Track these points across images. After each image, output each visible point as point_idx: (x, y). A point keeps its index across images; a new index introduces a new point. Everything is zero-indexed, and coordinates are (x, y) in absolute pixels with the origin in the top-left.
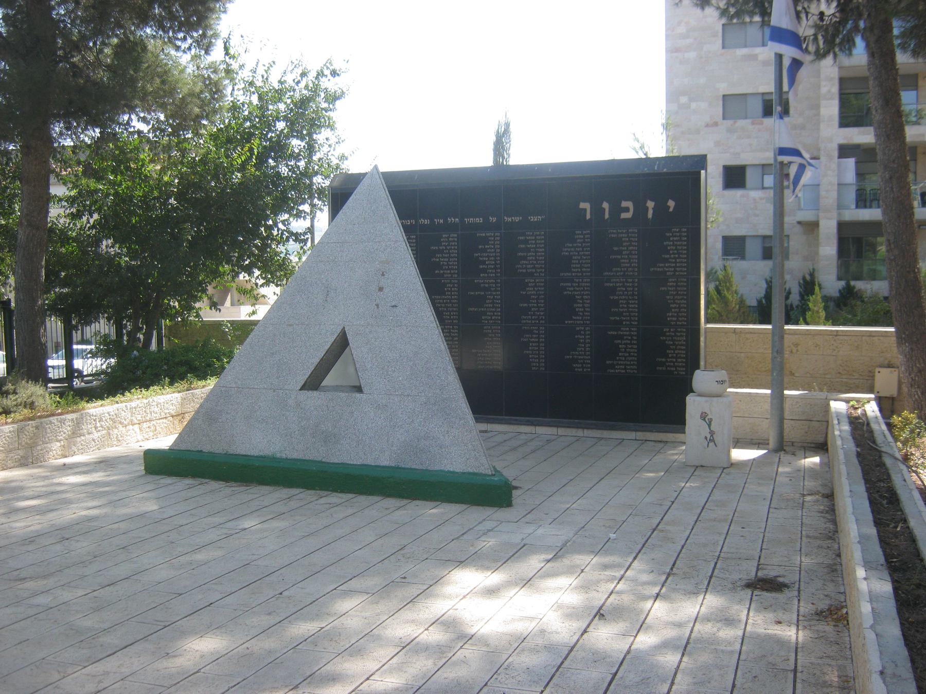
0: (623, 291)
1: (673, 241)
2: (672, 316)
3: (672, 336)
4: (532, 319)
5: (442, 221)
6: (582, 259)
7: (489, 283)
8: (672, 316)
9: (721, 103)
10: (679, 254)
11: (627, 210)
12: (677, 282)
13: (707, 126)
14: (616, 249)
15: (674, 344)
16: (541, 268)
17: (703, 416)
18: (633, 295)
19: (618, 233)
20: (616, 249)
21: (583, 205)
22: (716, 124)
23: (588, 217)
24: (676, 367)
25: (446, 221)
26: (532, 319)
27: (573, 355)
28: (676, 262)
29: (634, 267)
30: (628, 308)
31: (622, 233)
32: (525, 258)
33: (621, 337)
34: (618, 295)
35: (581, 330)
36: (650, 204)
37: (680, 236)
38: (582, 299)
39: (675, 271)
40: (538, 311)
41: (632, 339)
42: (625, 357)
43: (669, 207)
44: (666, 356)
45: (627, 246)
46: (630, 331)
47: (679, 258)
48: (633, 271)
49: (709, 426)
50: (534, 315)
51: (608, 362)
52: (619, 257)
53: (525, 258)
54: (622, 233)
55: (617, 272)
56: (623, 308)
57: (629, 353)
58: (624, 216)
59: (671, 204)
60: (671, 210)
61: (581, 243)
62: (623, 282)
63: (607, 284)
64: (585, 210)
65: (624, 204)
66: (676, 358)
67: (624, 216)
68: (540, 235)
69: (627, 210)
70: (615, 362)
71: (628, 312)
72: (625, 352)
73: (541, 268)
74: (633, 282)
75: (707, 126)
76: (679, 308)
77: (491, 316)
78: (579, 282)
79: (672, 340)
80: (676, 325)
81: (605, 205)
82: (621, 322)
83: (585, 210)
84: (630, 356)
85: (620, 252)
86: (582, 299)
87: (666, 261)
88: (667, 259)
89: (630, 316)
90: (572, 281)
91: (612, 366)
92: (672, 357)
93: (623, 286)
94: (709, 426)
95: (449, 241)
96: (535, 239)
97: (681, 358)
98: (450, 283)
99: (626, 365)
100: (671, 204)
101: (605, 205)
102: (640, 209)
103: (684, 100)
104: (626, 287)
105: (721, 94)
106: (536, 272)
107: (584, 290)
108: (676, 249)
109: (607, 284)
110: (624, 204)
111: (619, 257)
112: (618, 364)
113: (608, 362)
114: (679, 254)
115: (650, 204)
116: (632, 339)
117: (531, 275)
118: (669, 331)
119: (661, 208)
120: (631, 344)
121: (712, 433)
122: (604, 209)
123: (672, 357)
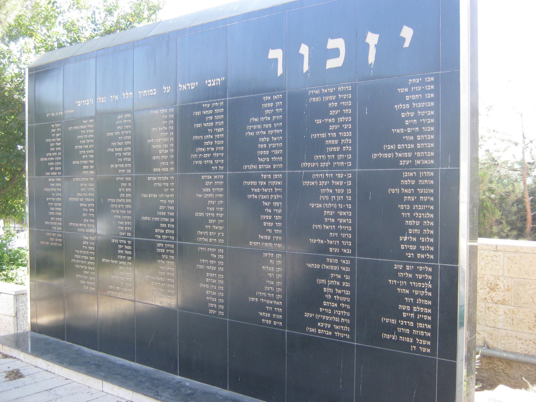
0: (330, 195)
1: (410, 102)
2: (409, 242)
3: (408, 280)
4: (209, 237)
6: (271, 141)
7: (162, 181)
8: (409, 242)
11: (335, 53)
14: (319, 121)
15: (411, 295)
16: (220, 158)
18: (345, 202)
19: (322, 95)
20: (319, 121)
23: (280, 71)
24: (414, 337)
26: (209, 237)
27: (259, 297)
28: (415, 142)
29: (347, 152)
30: (337, 223)
31: (329, 94)
32: (200, 143)
33: (325, 274)
34: (322, 202)
35: (269, 258)
36: (372, 39)
37: (423, 92)
38: (271, 207)
40: (216, 224)
41: (342, 280)
42: (333, 309)
43: (404, 40)
44: (398, 315)
45: (336, 117)
46: (340, 264)
47: (421, 132)
48: (345, 160)
50: (212, 230)
51: (307, 315)
52: (323, 135)
53: (200, 143)
54: (329, 94)
55: (320, 161)
56: (329, 223)
57: (339, 302)
58: (332, 63)
59: (407, 33)
60: (407, 44)
61: (270, 115)
62: (330, 179)
63: (306, 183)
64: (276, 60)
65: (332, 44)
66: (415, 321)
67: (332, 63)
68: (219, 107)
69: (335, 53)
70: (318, 316)
71: (337, 230)
72: (333, 300)
73: (220, 158)
74: (345, 179)
76: (422, 227)
77: (164, 229)
78: (267, 180)
79: (408, 287)
80: (415, 258)
81: (304, 50)
82: (324, 249)
83: (276, 60)
84: (339, 308)
85: (325, 128)
86: (271, 207)
88: (401, 135)
89: (340, 239)
90: (258, 178)
91: (313, 322)
92: (408, 319)
93: (330, 186)
96: (213, 114)
97: (422, 321)
98: (124, 181)
99: (333, 323)
100: (407, 33)
101: (304, 50)
102: (356, 48)
104: (334, 187)
106: (214, 164)
107: (274, 193)
108: (416, 117)
109: (306, 183)
110: (332, 44)
111: (323, 135)
112: (321, 320)
113: (307, 315)
115: (372, 39)
116: (342, 280)
117: (207, 168)
118: (404, 270)
119: (390, 43)
120: (341, 287)
122: (302, 56)
123: (408, 319)
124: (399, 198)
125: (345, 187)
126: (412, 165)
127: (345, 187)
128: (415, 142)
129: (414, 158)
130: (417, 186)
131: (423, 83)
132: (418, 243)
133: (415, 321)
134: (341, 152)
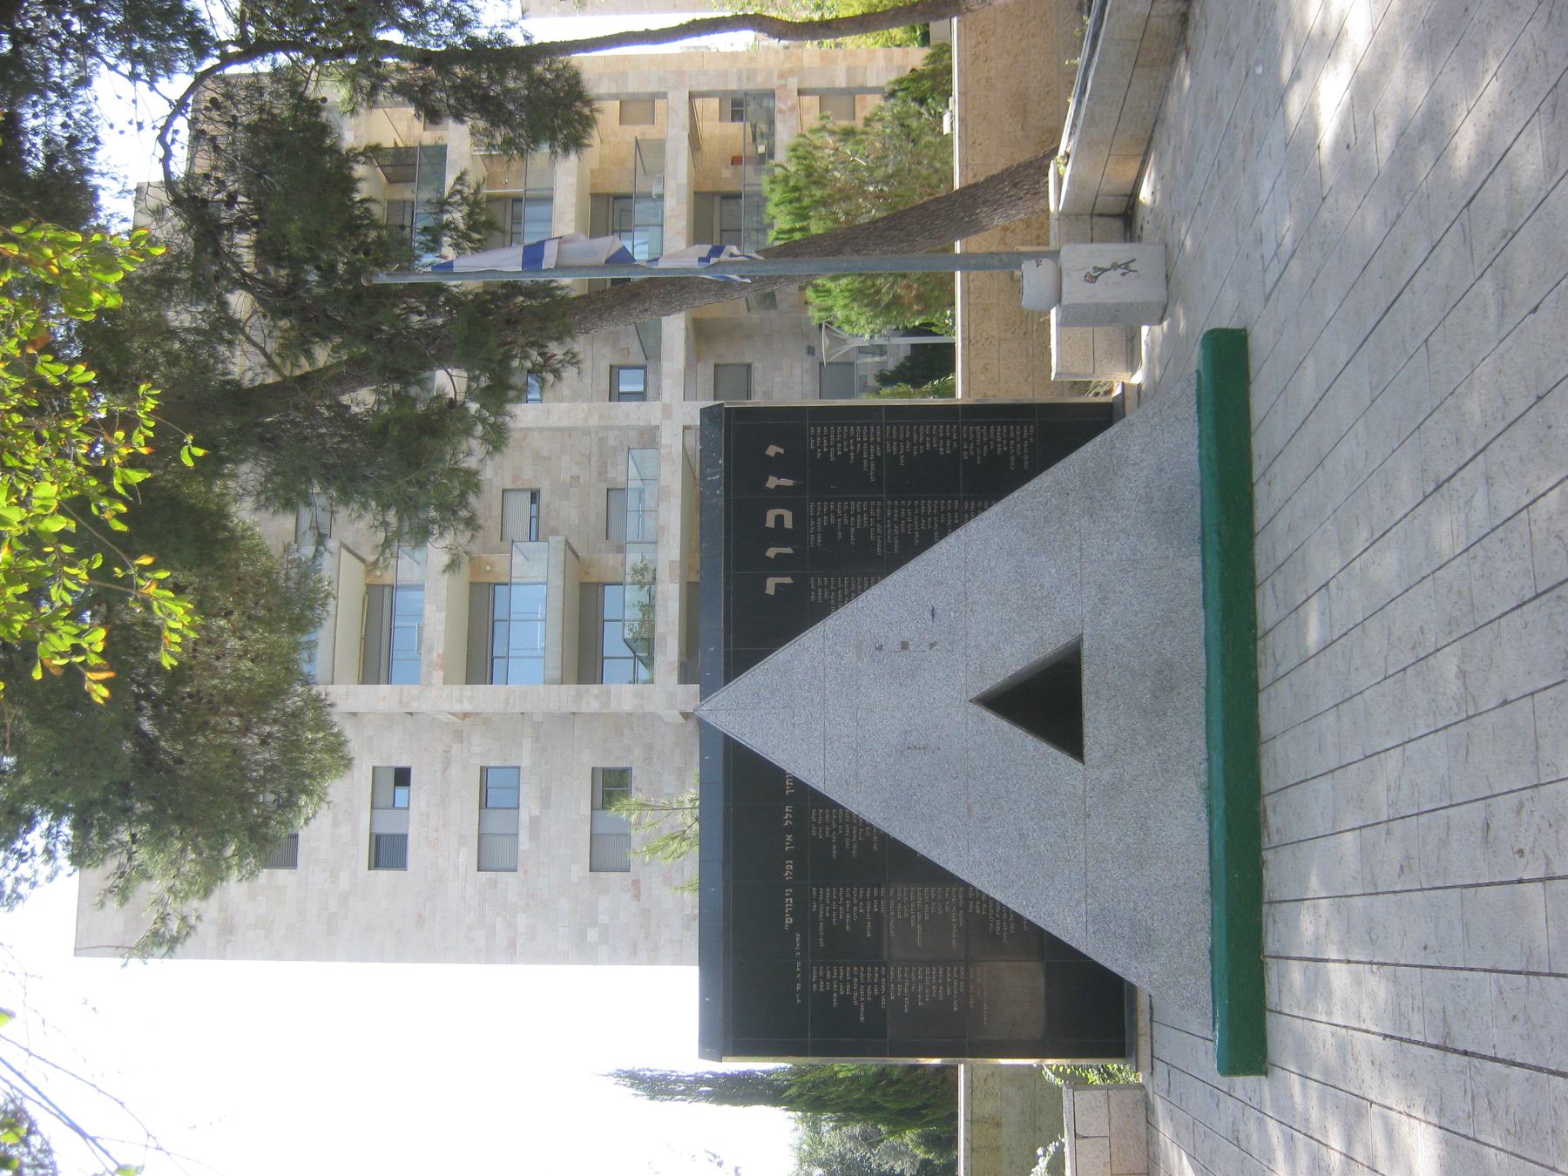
5: (789, 837)
9: (602, 874)
10: (848, 438)
11: (780, 519)
12: (891, 440)
13: (637, 897)
17: (1091, 279)
18: (912, 507)
19: (816, 533)
21: (770, 589)
22: (636, 883)
23: (788, 580)
25: (788, 830)
28: (862, 442)
30: (932, 515)
36: (772, 482)
39: (875, 443)
47: (854, 437)
49: (1105, 270)
59: (772, 450)
64: (777, 585)
67: (788, 523)
69: (780, 519)
74: (893, 508)
75: (637, 897)
79: (982, 446)
83: (777, 585)
85: (846, 529)
87: (859, 458)
89: (946, 512)
93: (899, 523)
94: (1105, 270)
95: (824, 824)
100: (772, 450)
101: (771, 553)
102: (779, 498)
103: (593, 935)
104: (900, 519)
105: (588, 874)
114: (848, 438)
115: (772, 482)
121: (1115, 266)
124: (908, 455)
125: (899, 508)
126: (881, 444)
127: (899, 508)
128: (862, 442)
129: (875, 443)
130: (898, 440)
131: (815, 436)
132: (944, 438)
133: (1009, 439)
134: (868, 512)
